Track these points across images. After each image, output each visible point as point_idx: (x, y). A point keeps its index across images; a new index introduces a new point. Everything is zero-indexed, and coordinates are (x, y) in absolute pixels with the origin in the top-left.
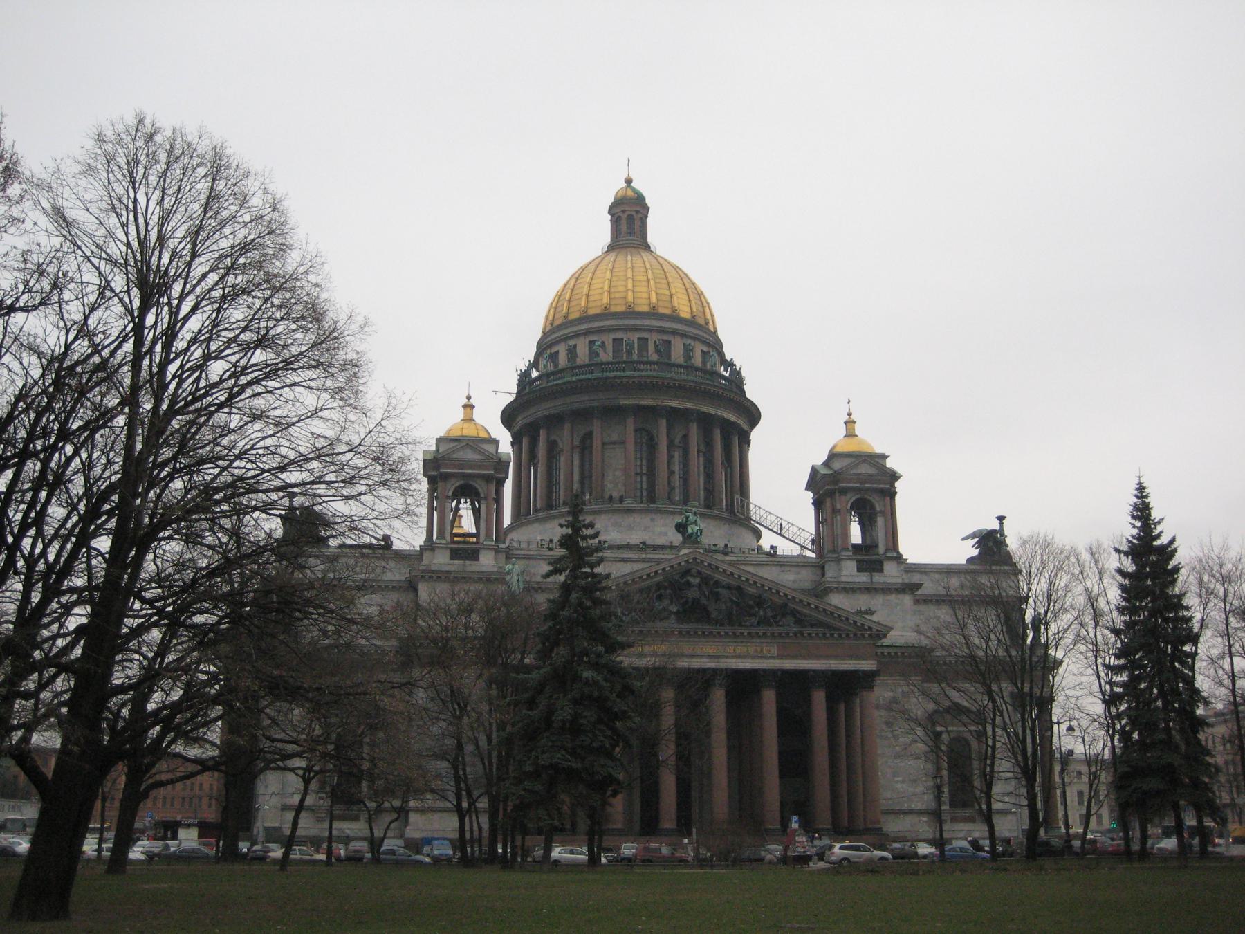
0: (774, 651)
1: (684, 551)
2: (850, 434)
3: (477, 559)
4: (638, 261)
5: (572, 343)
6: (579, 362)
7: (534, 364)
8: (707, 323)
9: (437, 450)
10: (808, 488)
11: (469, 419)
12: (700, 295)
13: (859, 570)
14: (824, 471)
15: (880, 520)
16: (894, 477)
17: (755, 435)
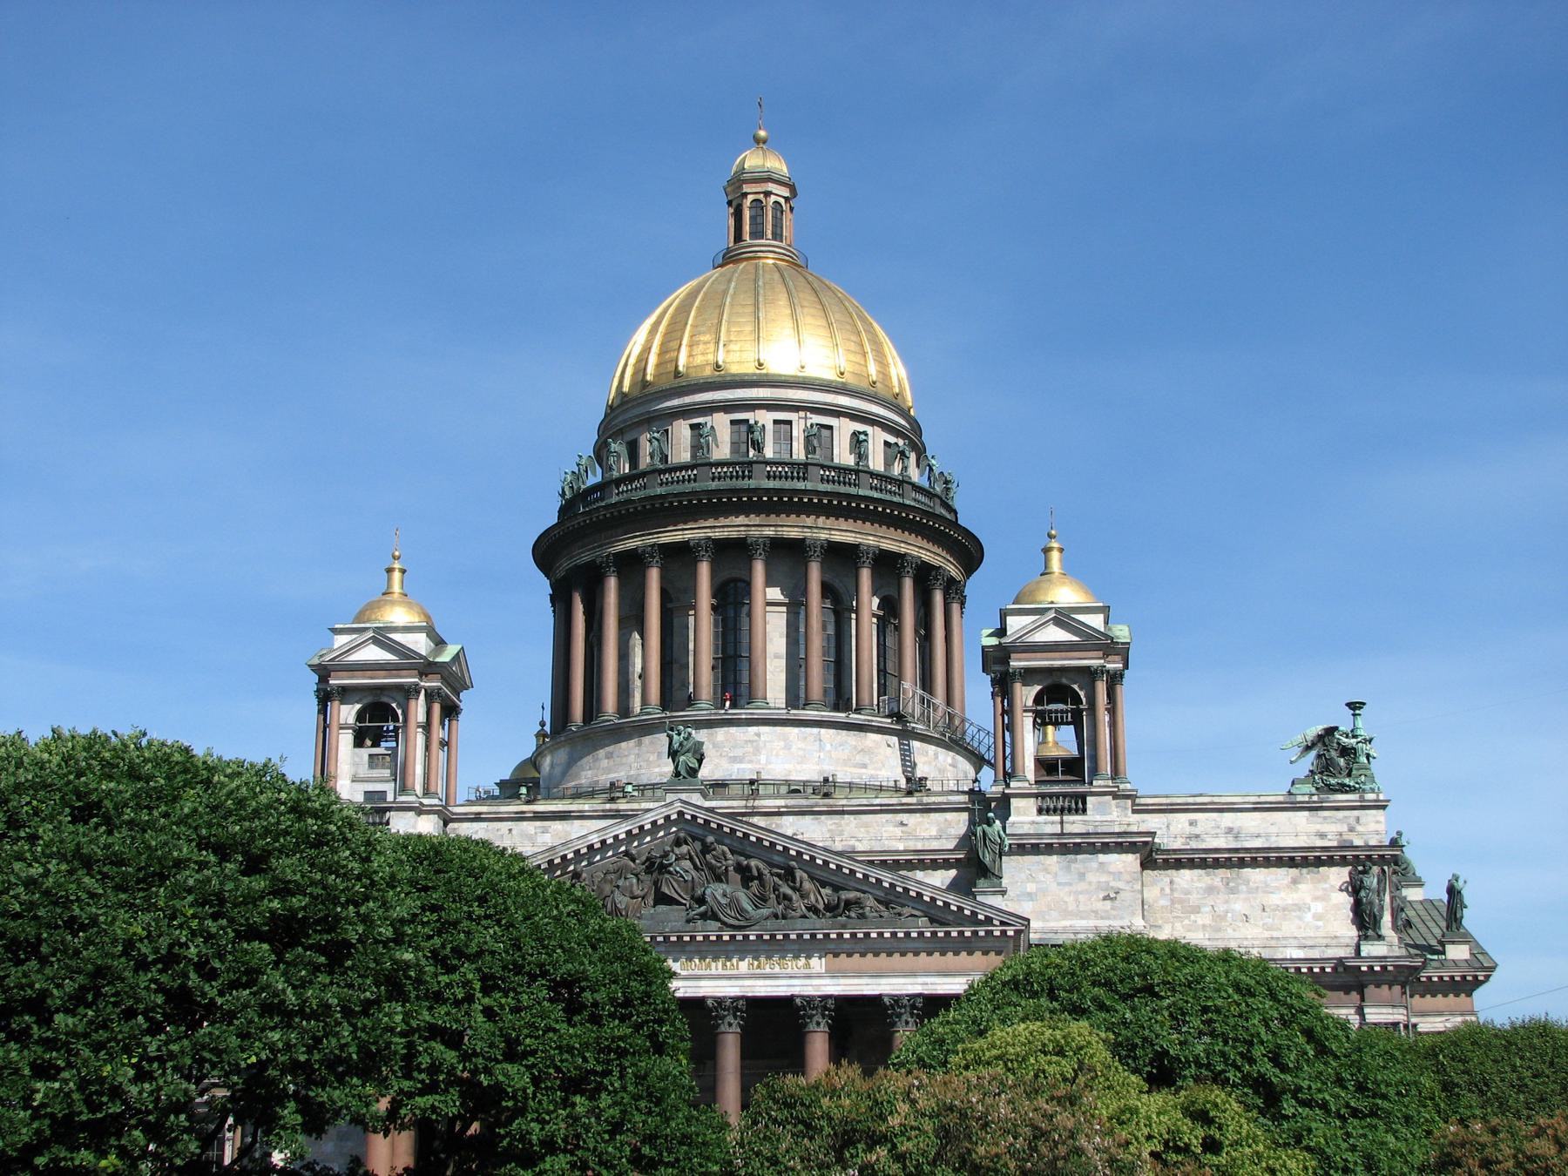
5: (629, 437)
13: (1040, 811)
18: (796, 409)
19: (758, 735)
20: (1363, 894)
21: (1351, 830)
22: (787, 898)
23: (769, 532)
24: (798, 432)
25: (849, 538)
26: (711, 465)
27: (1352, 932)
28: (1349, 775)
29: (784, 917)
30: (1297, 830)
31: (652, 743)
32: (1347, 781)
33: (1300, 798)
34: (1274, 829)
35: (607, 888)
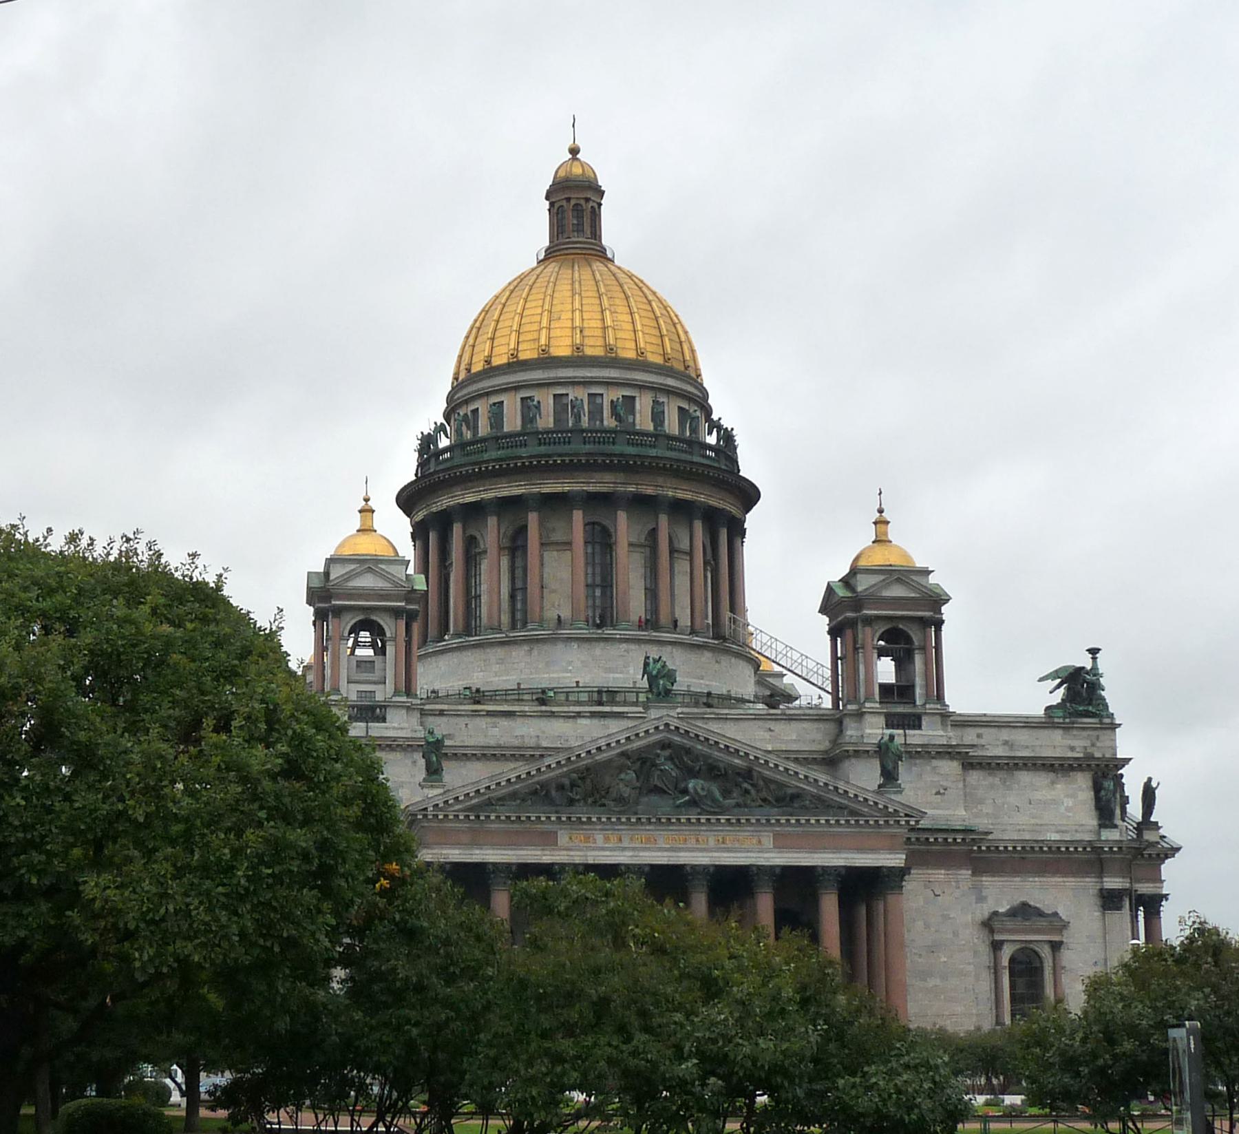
0: (768, 841)
1: (653, 714)
2: (880, 540)
3: (383, 719)
4: (586, 274)
6: (507, 429)
7: (440, 429)
8: (687, 368)
9: (327, 574)
10: (823, 610)
11: (366, 530)
12: (674, 323)
14: (841, 592)
15: (918, 660)
16: (937, 600)
17: (752, 520)
18: (642, 387)
19: (627, 651)
20: (1103, 793)
21: (1093, 745)
22: (747, 792)
23: (632, 489)
24: (644, 404)
25: (688, 496)
26: (583, 431)
27: (1095, 822)
28: (1089, 704)
29: (746, 806)
30: (1056, 744)
31: (539, 654)
32: (1090, 708)
33: (1056, 720)
34: (1038, 743)
35: (607, 779)
